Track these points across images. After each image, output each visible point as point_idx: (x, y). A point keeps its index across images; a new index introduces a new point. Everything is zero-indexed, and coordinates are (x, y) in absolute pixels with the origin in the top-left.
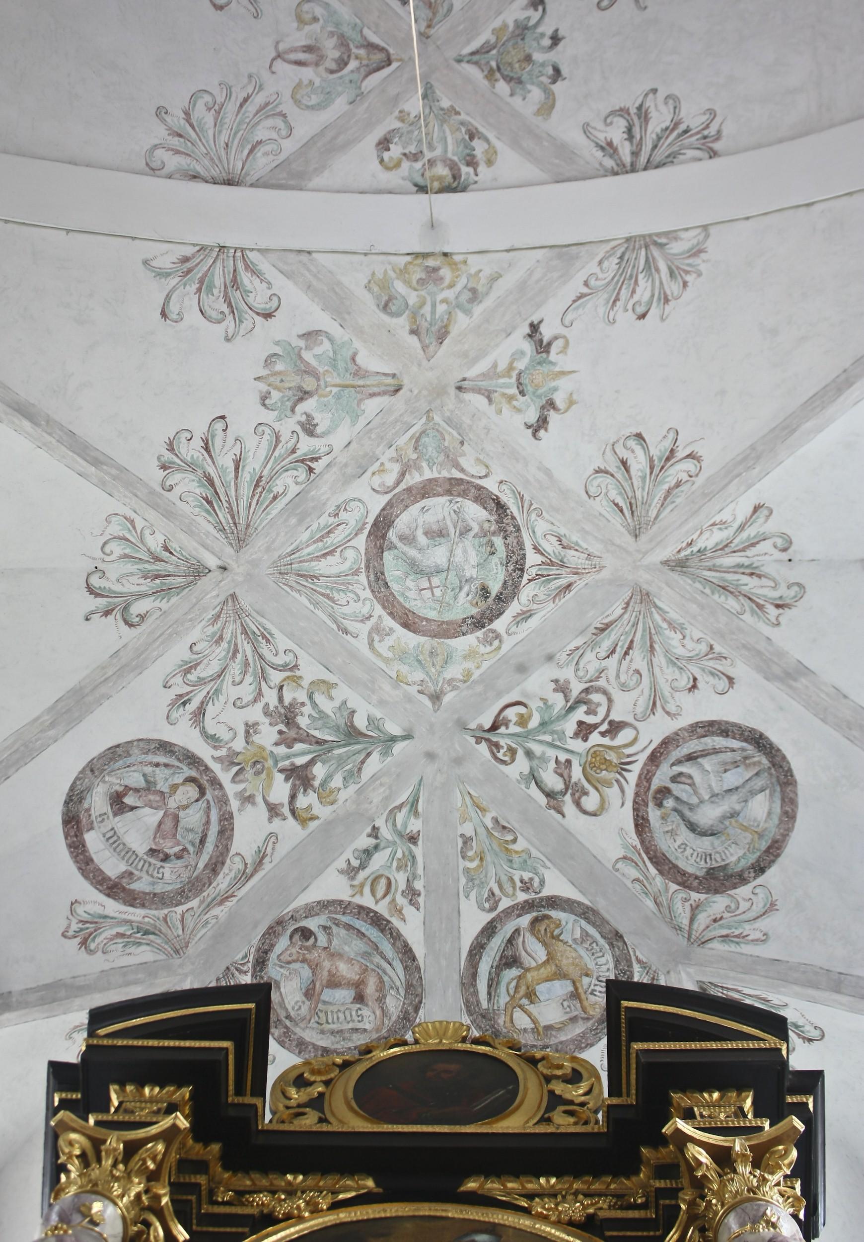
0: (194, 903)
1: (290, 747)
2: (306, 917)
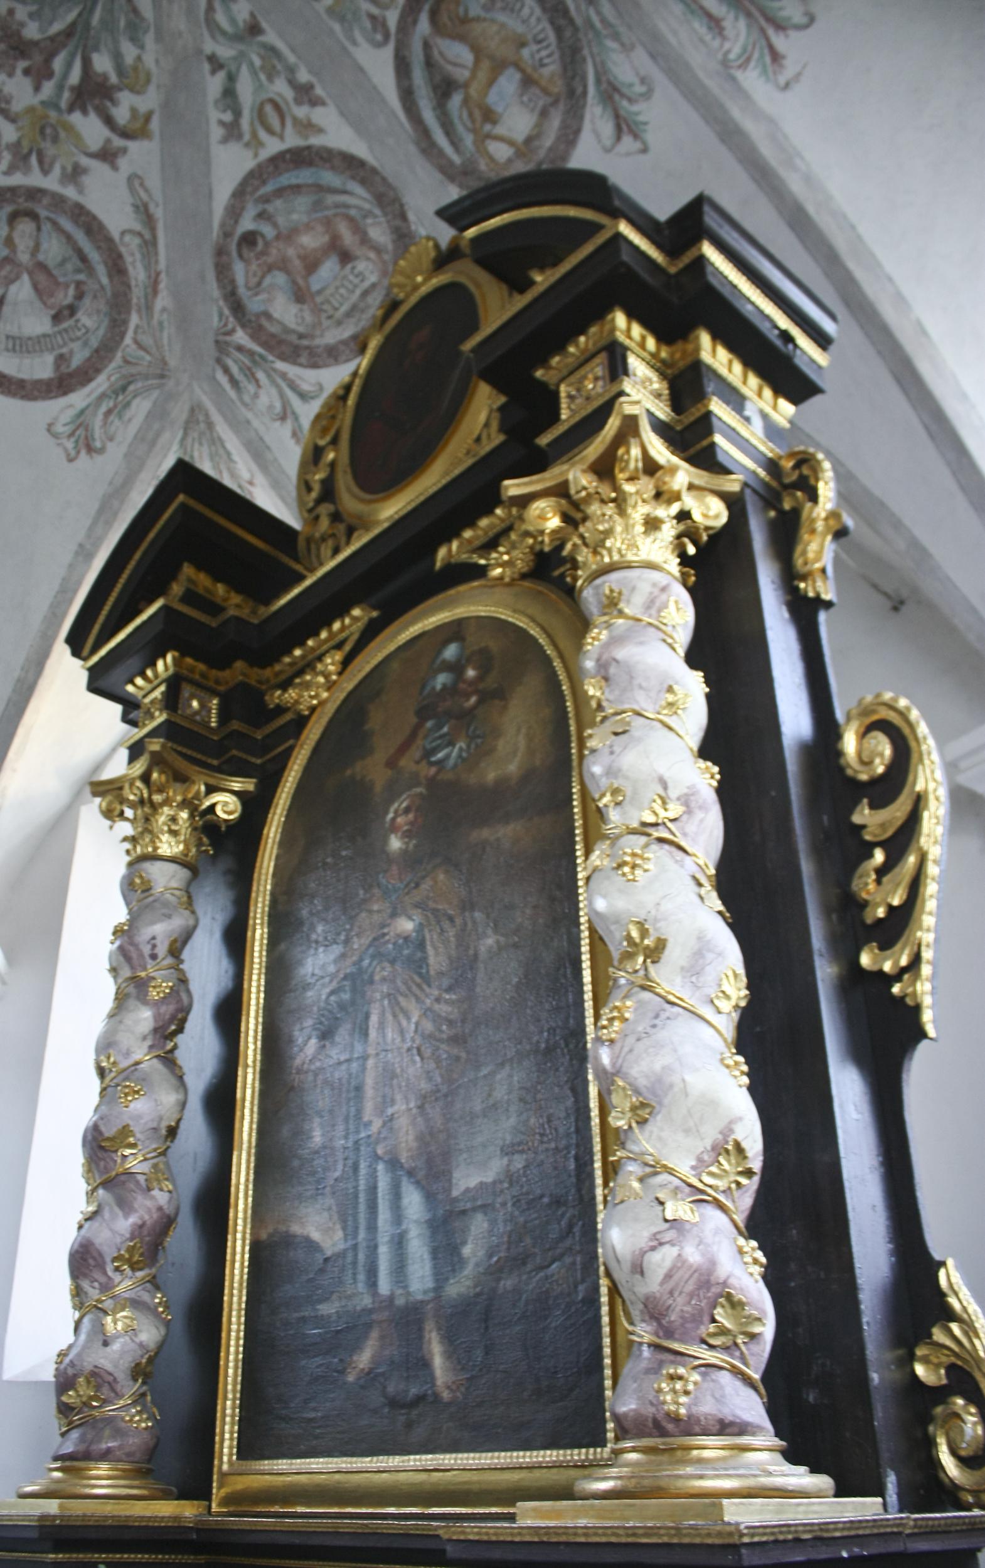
0: (134, 319)
1: (50, 75)
2: (236, 222)
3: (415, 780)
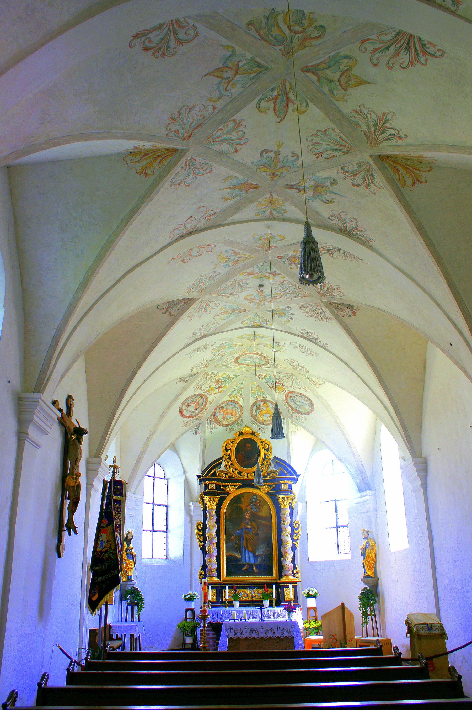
3: (249, 511)
